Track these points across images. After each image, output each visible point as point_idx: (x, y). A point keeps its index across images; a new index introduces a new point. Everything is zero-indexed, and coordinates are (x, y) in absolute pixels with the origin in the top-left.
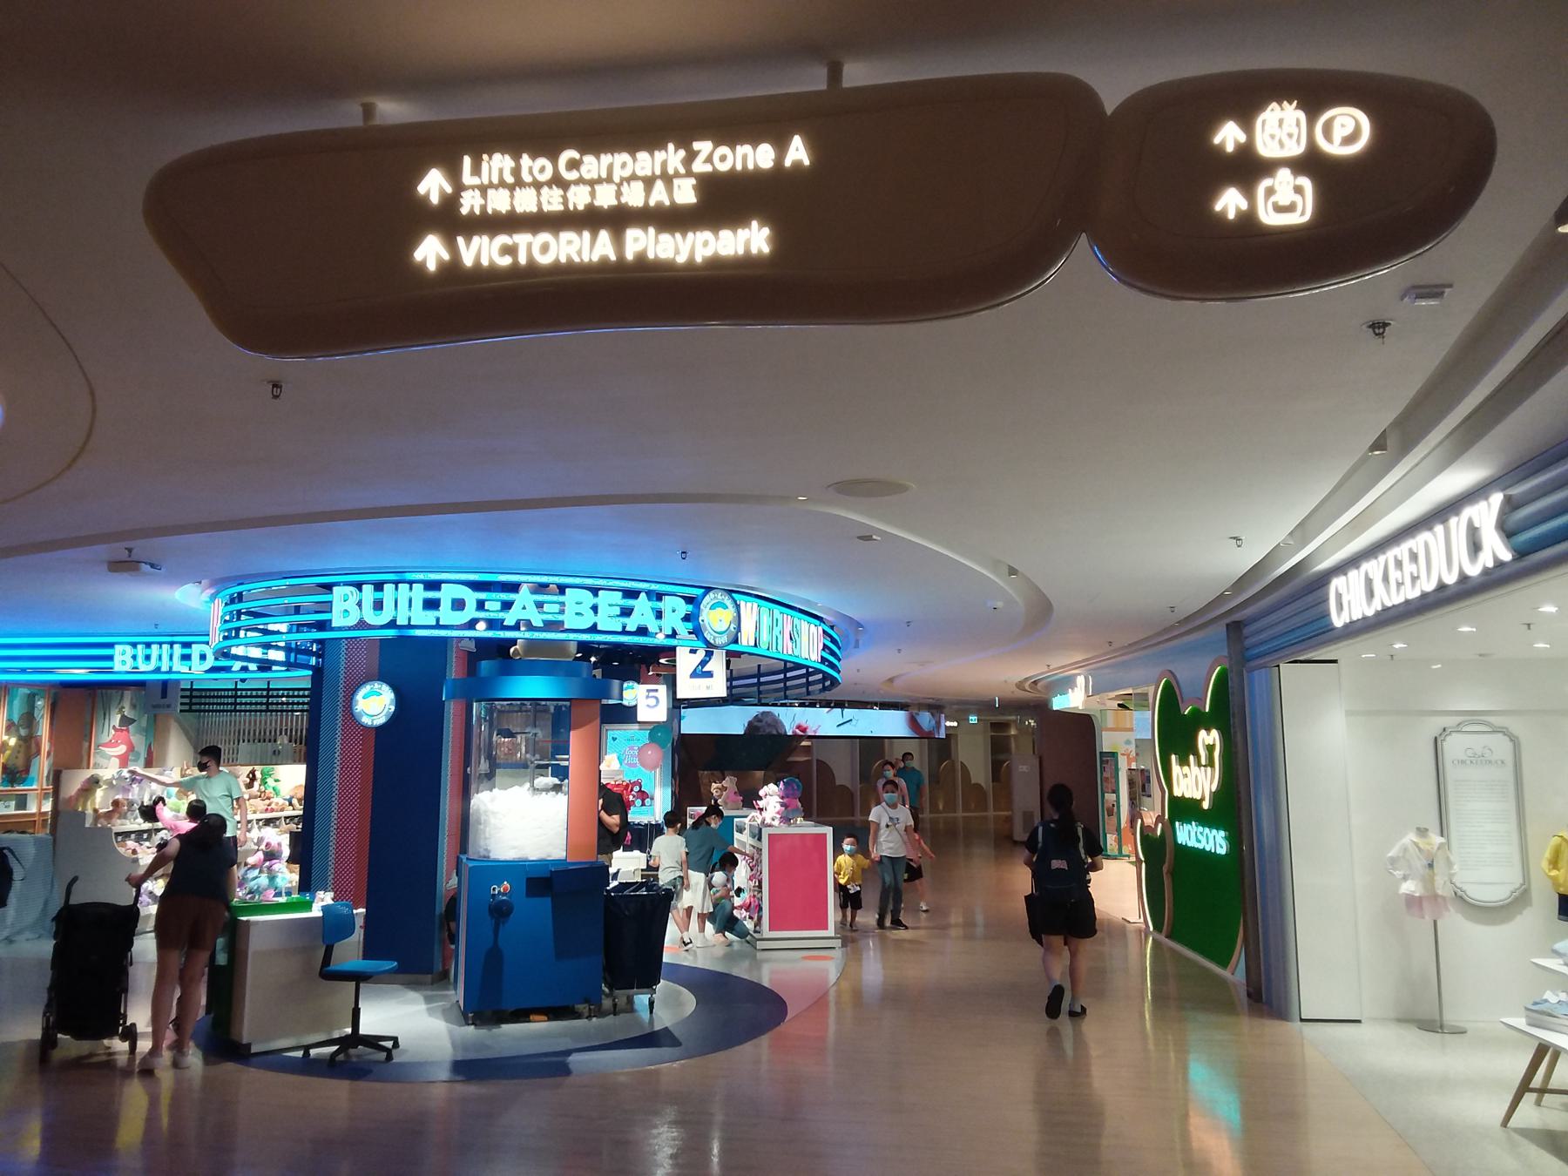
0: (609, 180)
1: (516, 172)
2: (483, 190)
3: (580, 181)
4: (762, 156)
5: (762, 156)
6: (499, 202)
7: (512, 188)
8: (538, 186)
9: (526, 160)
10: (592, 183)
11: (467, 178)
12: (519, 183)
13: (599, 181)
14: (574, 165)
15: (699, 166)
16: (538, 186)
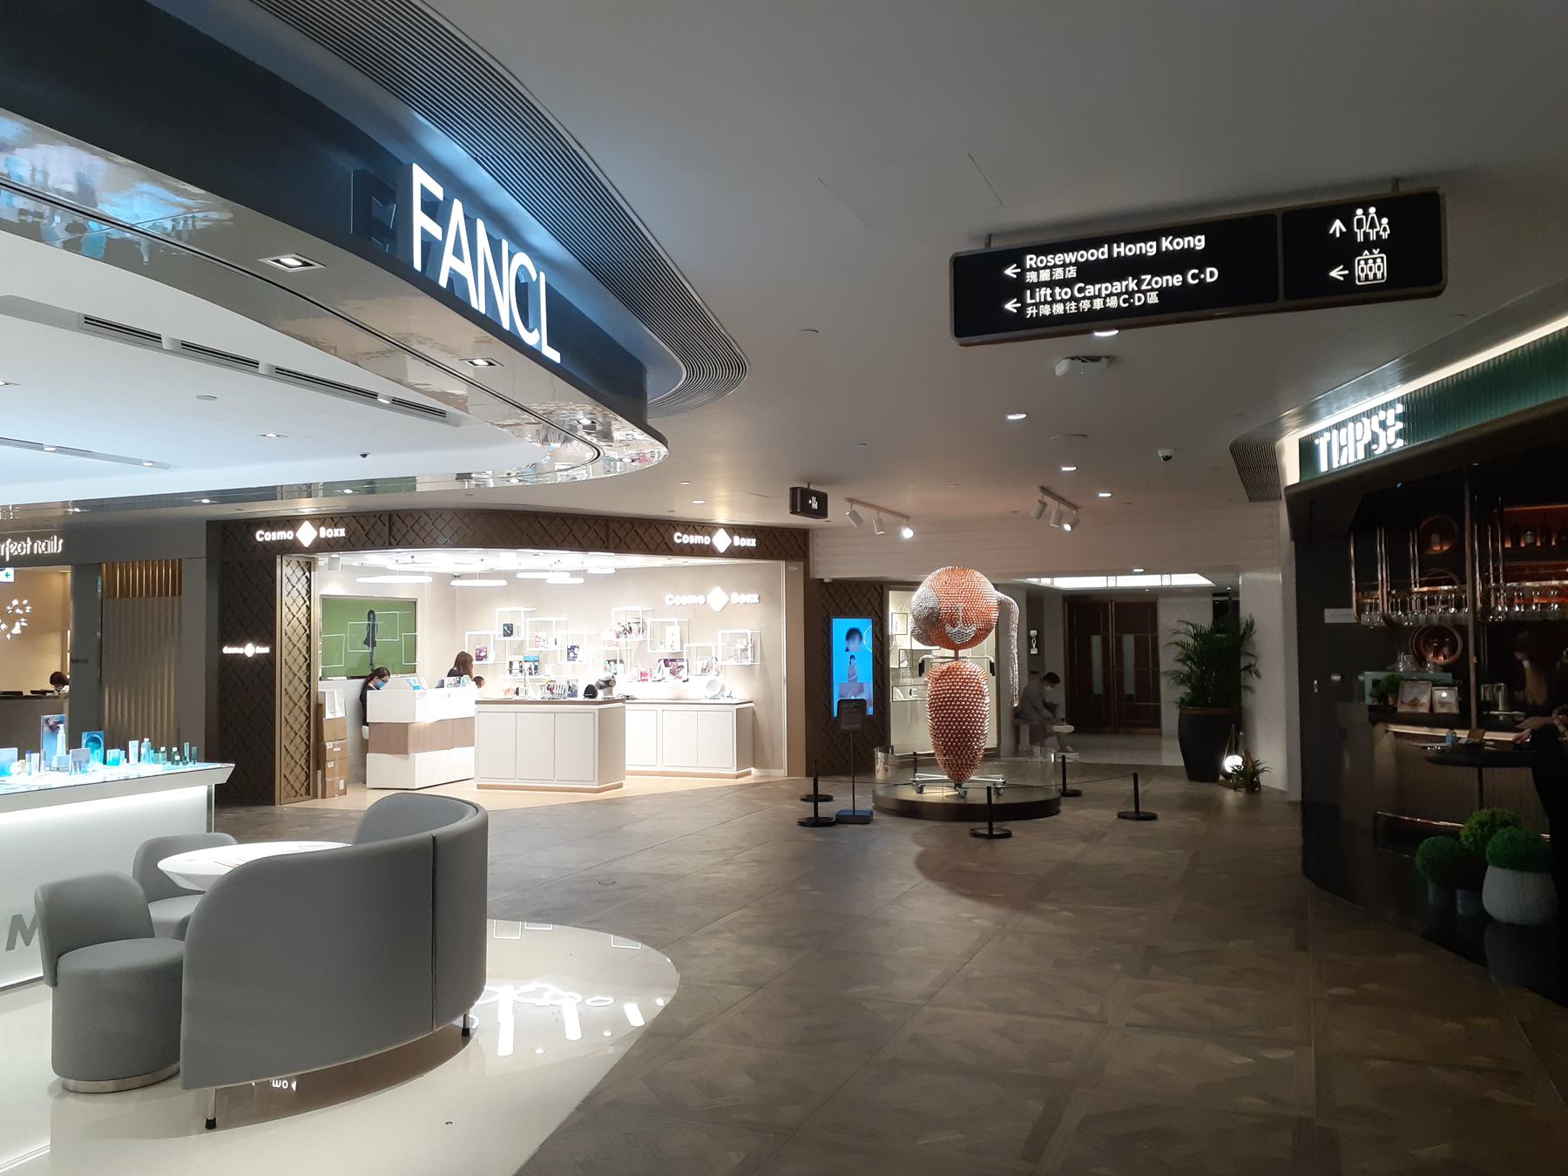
0: (1099, 296)
1: (1052, 295)
2: (1037, 305)
3: (1085, 298)
4: (1176, 280)
5: (1176, 280)
6: (1045, 310)
7: (1051, 303)
8: (1063, 301)
9: (1057, 290)
10: (1091, 298)
11: (1029, 301)
12: (1054, 301)
13: (1095, 297)
14: (1080, 290)
15: (1144, 287)
16: (1063, 301)
